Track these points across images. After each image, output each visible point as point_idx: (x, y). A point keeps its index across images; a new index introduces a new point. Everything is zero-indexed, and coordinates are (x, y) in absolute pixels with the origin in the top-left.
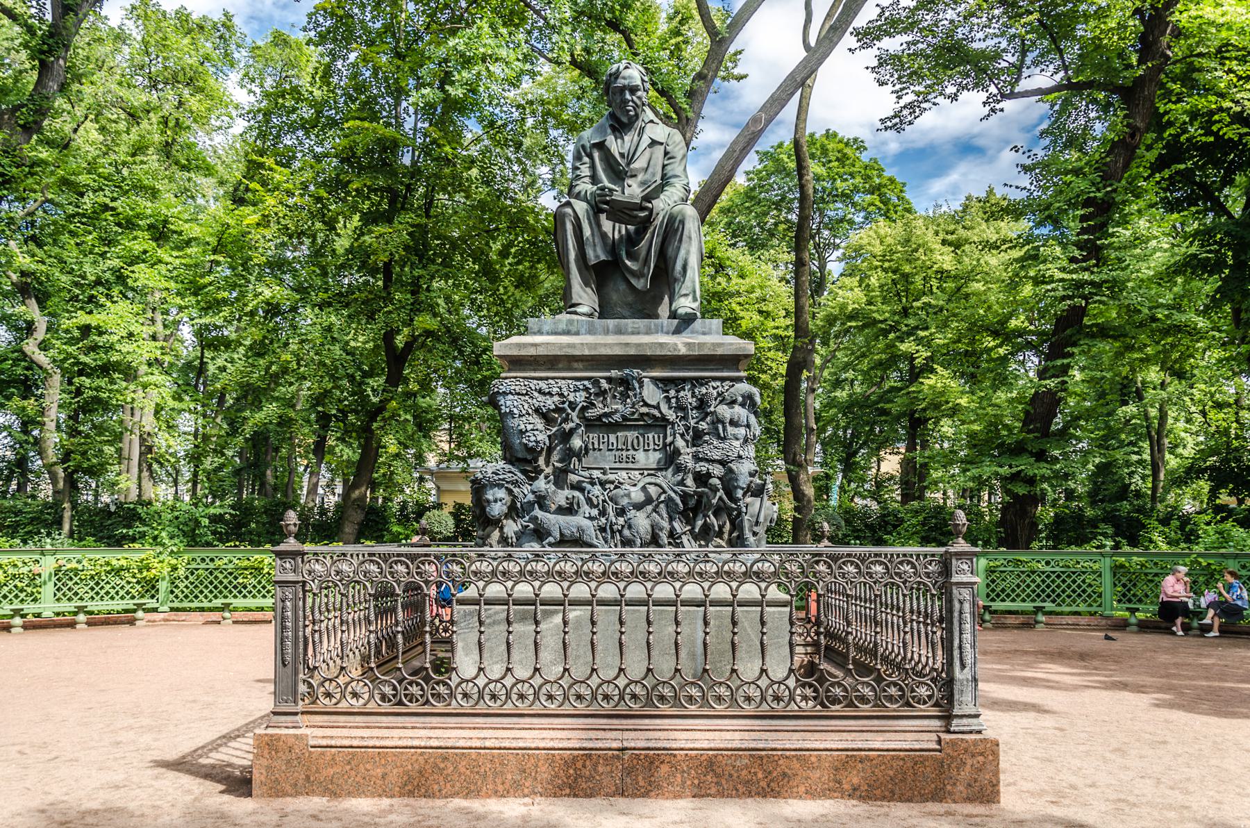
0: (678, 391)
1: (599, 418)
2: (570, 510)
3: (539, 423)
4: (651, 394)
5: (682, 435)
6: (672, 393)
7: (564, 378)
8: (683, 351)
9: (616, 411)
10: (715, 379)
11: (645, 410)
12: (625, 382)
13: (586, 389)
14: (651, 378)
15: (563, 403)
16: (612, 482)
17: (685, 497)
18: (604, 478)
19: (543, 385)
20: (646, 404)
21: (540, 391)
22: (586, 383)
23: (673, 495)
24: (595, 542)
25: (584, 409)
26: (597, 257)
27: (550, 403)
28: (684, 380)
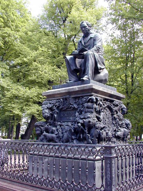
0: (78, 100)
1: (62, 108)
2: (52, 133)
3: (47, 111)
4: (72, 101)
5: (78, 112)
6: (77, 101)
7: (55, 100)
8: (77, 89)
9: (65, 107)
10: (85, 96)
11: (71, 106)
12: (66, 99)
13: (59, 102)
14: (72, 97)
15: (54, 105)
16: (63, 125)
17: (75, 129)
18: (61, 124)
19: (51, 101)
20: (71, 104)
21: (50, 103)
22: (59, 100)
23: (71, 128)
24: (56, 141)
25: (58, 107)
26: (73, 68)
27: (51, 106)
28: (79, 97)
